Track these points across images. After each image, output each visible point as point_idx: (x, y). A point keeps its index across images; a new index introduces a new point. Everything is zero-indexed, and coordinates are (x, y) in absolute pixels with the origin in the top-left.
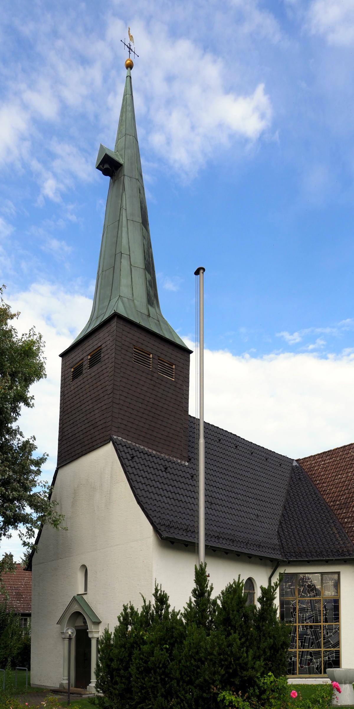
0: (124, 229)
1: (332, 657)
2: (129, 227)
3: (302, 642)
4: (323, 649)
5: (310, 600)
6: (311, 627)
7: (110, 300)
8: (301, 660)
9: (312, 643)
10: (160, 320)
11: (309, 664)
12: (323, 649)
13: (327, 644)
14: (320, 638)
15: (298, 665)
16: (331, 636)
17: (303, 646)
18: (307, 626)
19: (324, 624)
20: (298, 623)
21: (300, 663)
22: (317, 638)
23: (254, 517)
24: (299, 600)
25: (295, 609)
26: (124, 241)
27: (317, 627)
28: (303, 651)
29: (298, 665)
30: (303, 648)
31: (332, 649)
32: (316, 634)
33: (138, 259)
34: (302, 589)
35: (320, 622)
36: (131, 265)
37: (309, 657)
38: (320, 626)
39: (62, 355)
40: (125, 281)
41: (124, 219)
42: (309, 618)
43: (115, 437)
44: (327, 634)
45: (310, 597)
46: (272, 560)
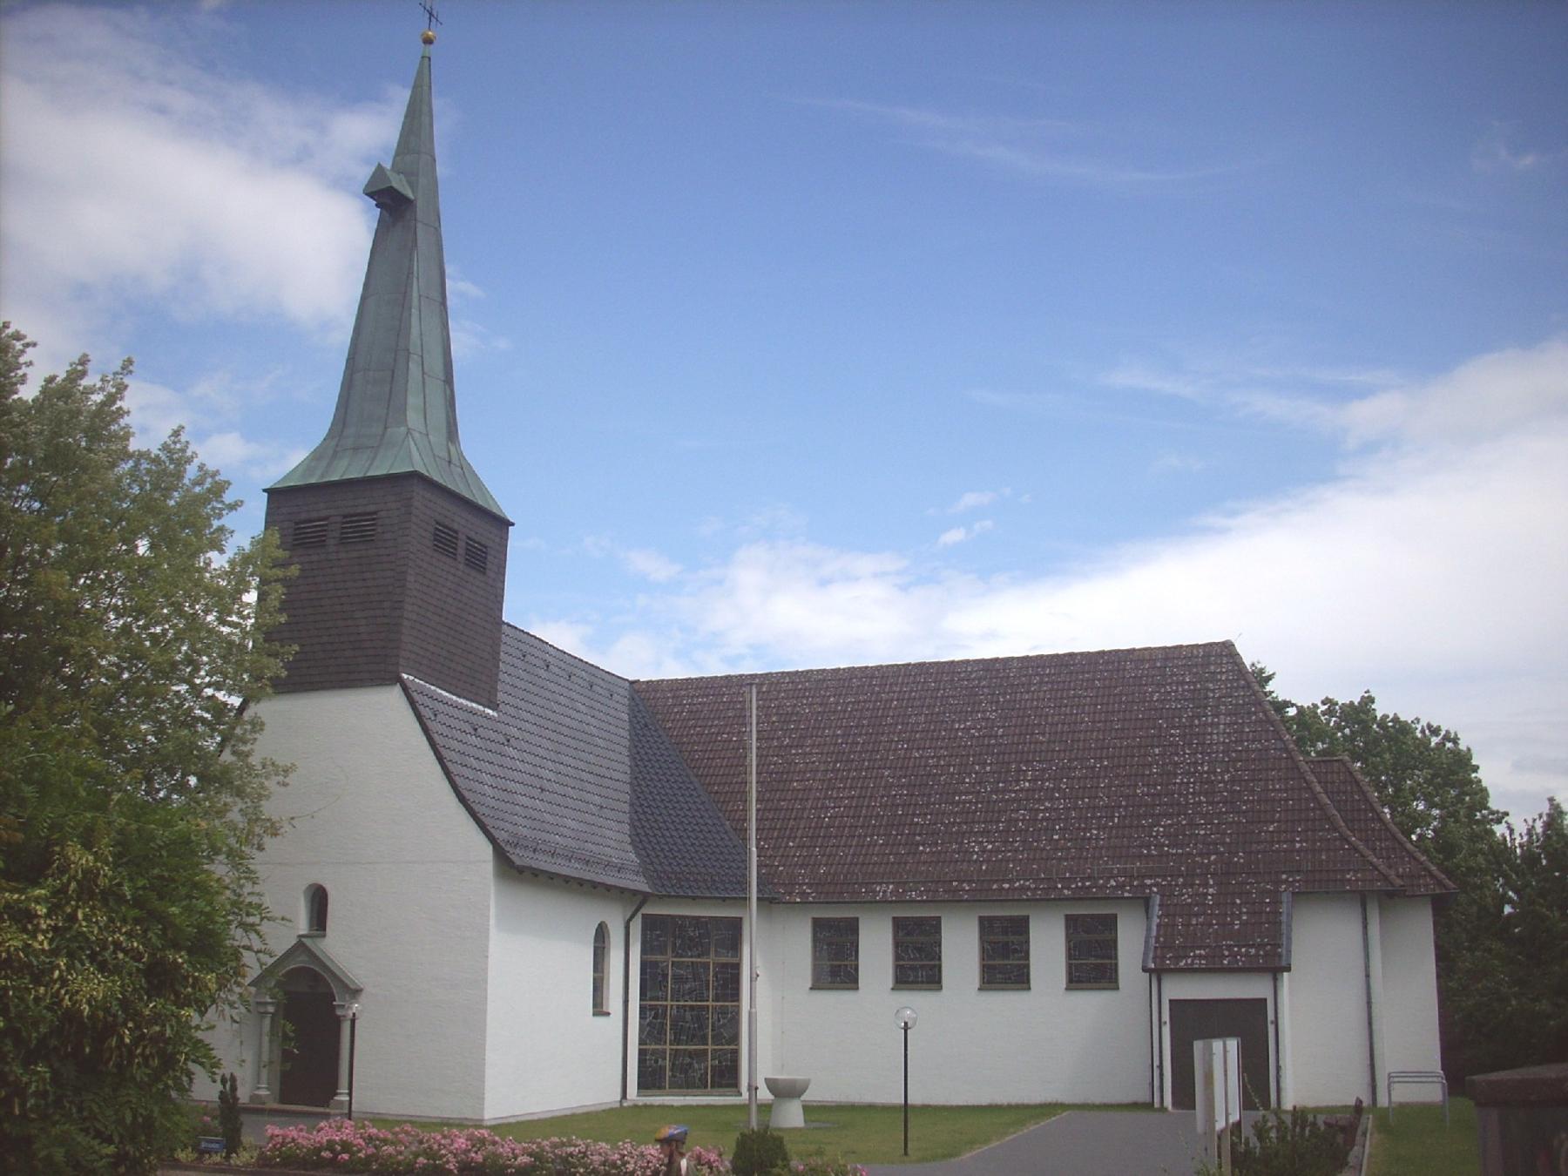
0: (414, 311)
1: (726, 1060)
2: (423, 309)
3: (675, 1034)
4: (710, 1047)
5: (692, 962)
6: (692, 1008)
7: (386, 428)
8: (673, 1064)
9: (694, 1036)
10: (465, 470)
11: (686, 1072)
12: (710, 1047)
13: (717, 1039)
14: (707, 1027)
15: (668, 1073)
16: (724, 1025)
17: (677, 1041)
18: (685, 1006)
19: (714, 1004)
20: (672, 1000)
21: (672, 1070)
22: (702, 1027)
23: (594, 809)
24: (673, 963)
25: (665, 976)
26: (415, 331)
27: (702, 1008)
28: (677, 1050)
29: (668, 1073)
30: (678, 1045)
31: (726, 1047)
32: (700, 1019)
33: (435, 364)
34: (678, 942)
35: (708, 1001)
36: (423, 373)
37: (688, 1060)
38: (708, 1006)
39: (271, 492)
40: (413, 400)
41: (415, 295)
42: (689, 993)
43: (405, 676)
44: (719, 1021)
45: (692, 957)
46: (635, 893)
